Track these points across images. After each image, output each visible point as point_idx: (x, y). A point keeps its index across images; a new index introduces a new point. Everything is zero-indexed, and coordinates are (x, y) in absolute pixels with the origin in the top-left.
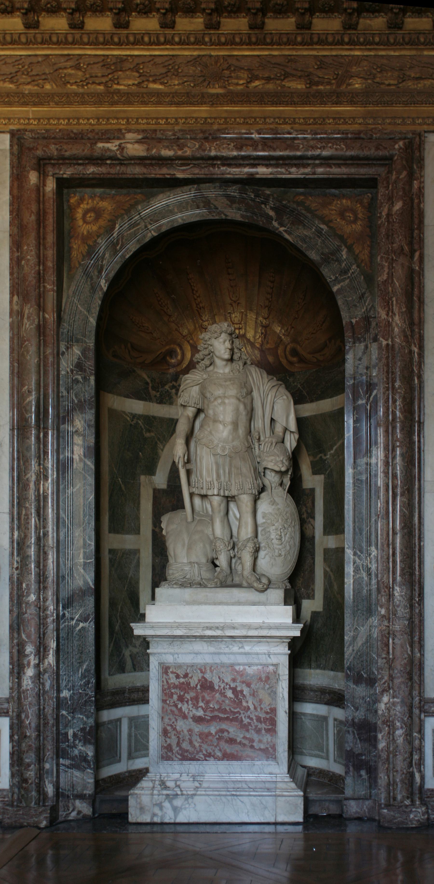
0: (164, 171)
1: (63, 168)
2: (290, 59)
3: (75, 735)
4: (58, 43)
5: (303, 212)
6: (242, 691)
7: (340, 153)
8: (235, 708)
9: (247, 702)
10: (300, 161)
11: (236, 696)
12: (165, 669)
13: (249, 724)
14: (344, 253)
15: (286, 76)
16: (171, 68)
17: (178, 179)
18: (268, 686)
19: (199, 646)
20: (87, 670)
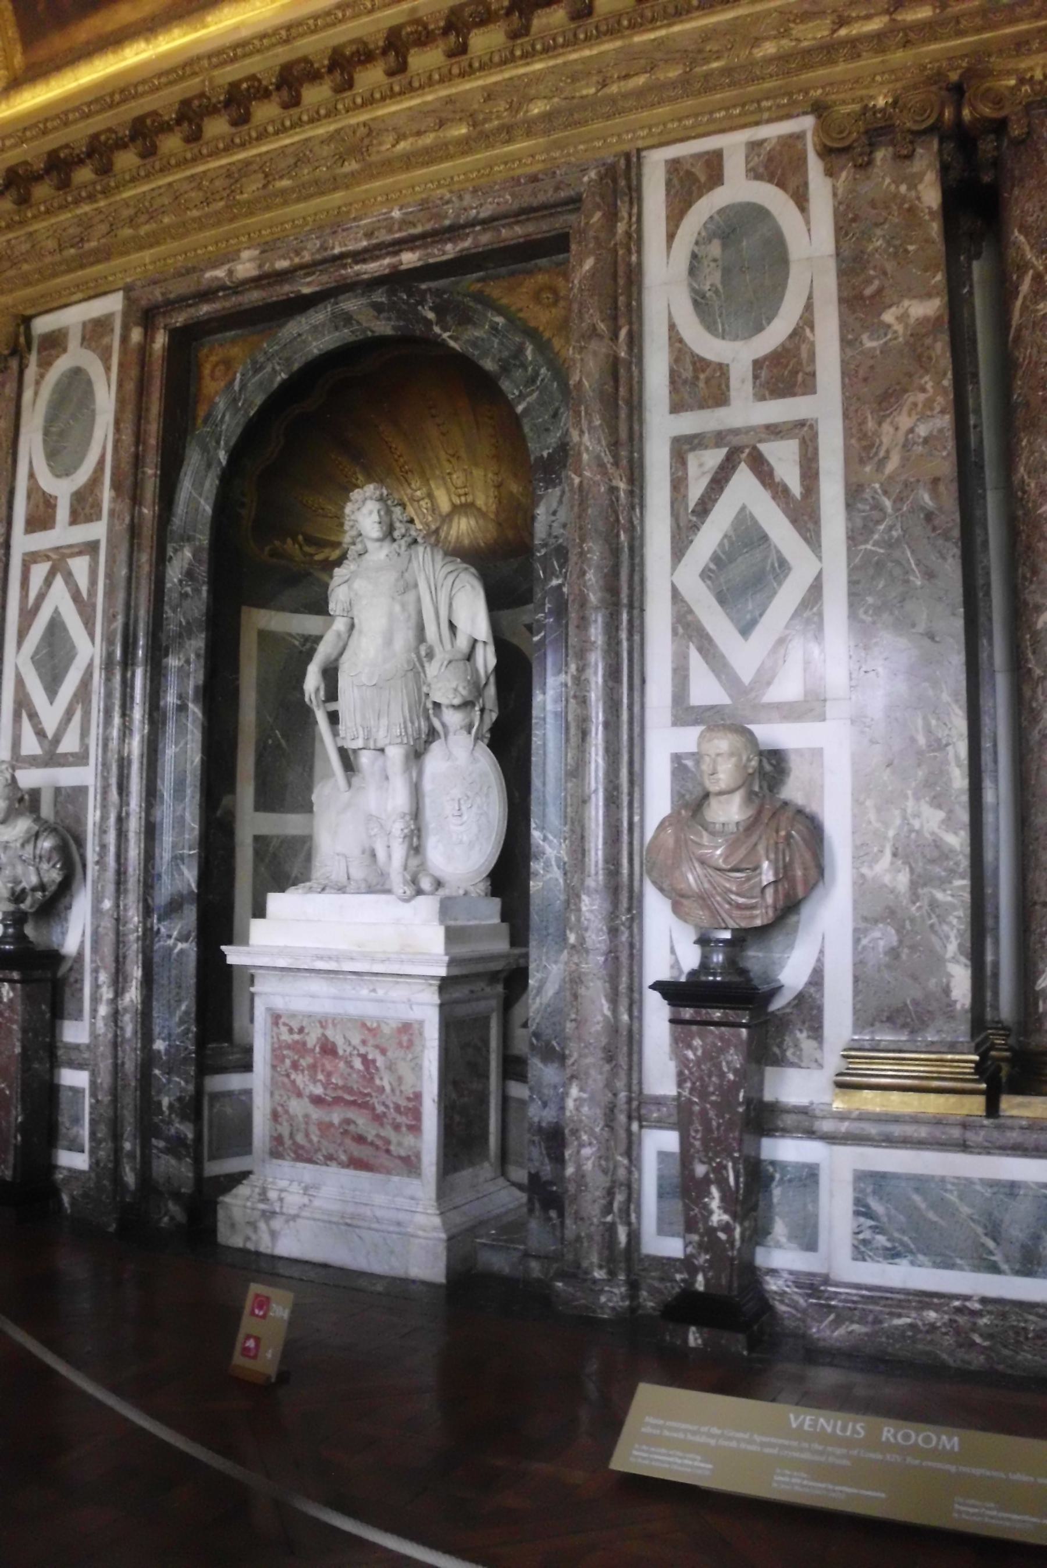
0: (287, 288)
1: (174, 314)
2: (450, 100)
3: (171, 1106)
4: (178, 165)
5: (471, 304)
6: (374, 1061)
7: (503, 208)
8: (365, 1087)
9: (381, 1079)
10: (454, 232)
11: (367, 1068)
12: (276, 1018)
13: (384, 1113)
14: (529, 352)
15: (441, 124)
16: (301, 157)
17: (305, 296)
18: (410, 1056)
19: (317, 986)
20: (187, 1013)
